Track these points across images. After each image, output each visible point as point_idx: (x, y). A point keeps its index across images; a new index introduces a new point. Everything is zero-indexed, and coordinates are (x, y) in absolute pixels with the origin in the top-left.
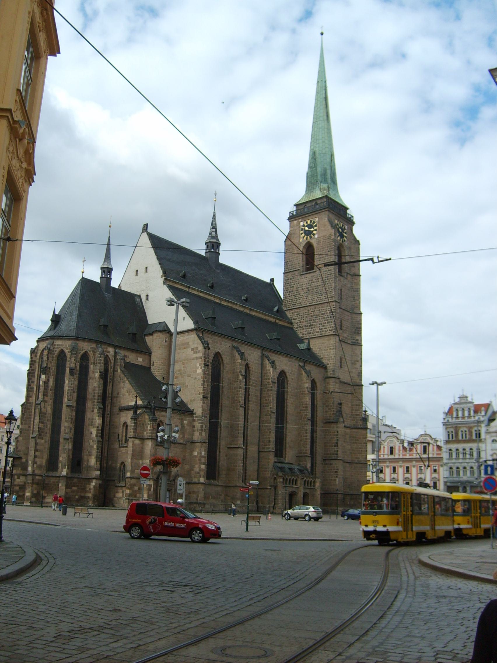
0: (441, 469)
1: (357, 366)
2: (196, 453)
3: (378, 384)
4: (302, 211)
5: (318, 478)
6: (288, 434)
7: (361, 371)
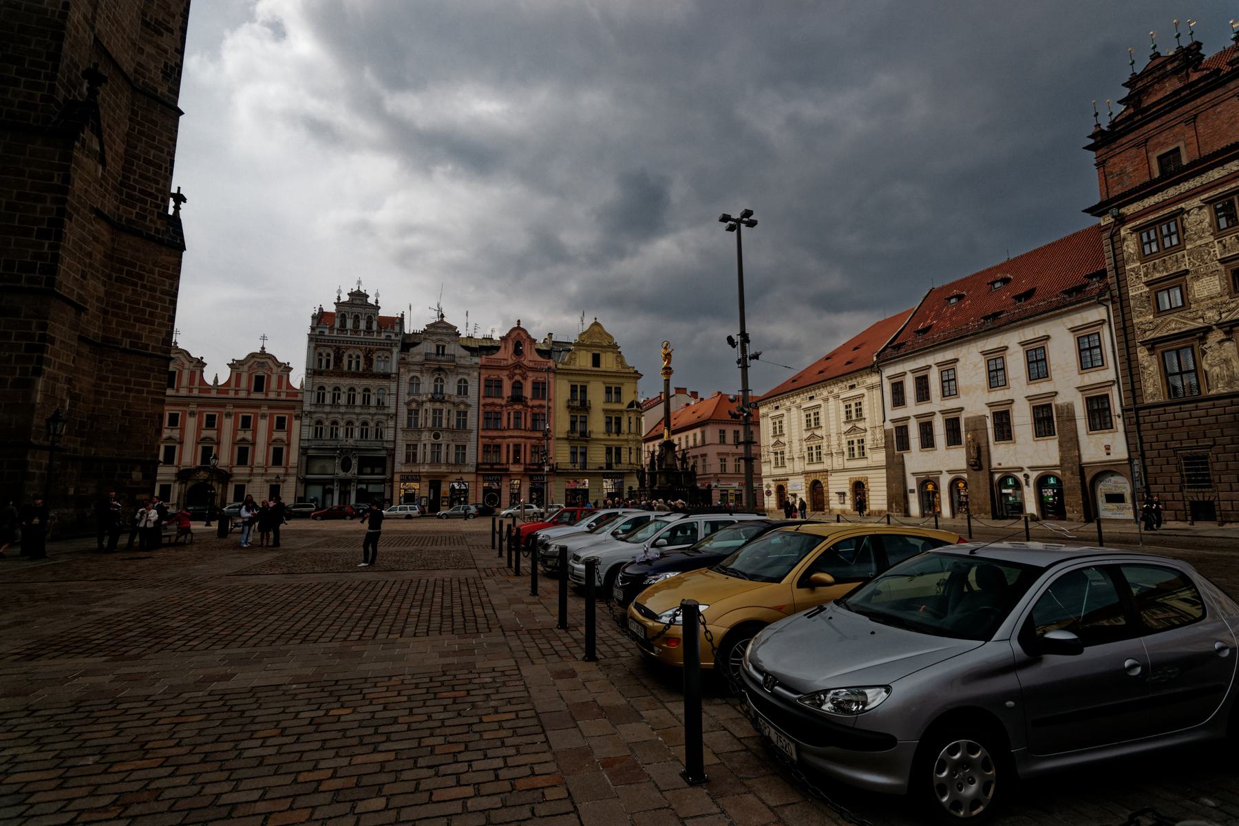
7: (179, 66)
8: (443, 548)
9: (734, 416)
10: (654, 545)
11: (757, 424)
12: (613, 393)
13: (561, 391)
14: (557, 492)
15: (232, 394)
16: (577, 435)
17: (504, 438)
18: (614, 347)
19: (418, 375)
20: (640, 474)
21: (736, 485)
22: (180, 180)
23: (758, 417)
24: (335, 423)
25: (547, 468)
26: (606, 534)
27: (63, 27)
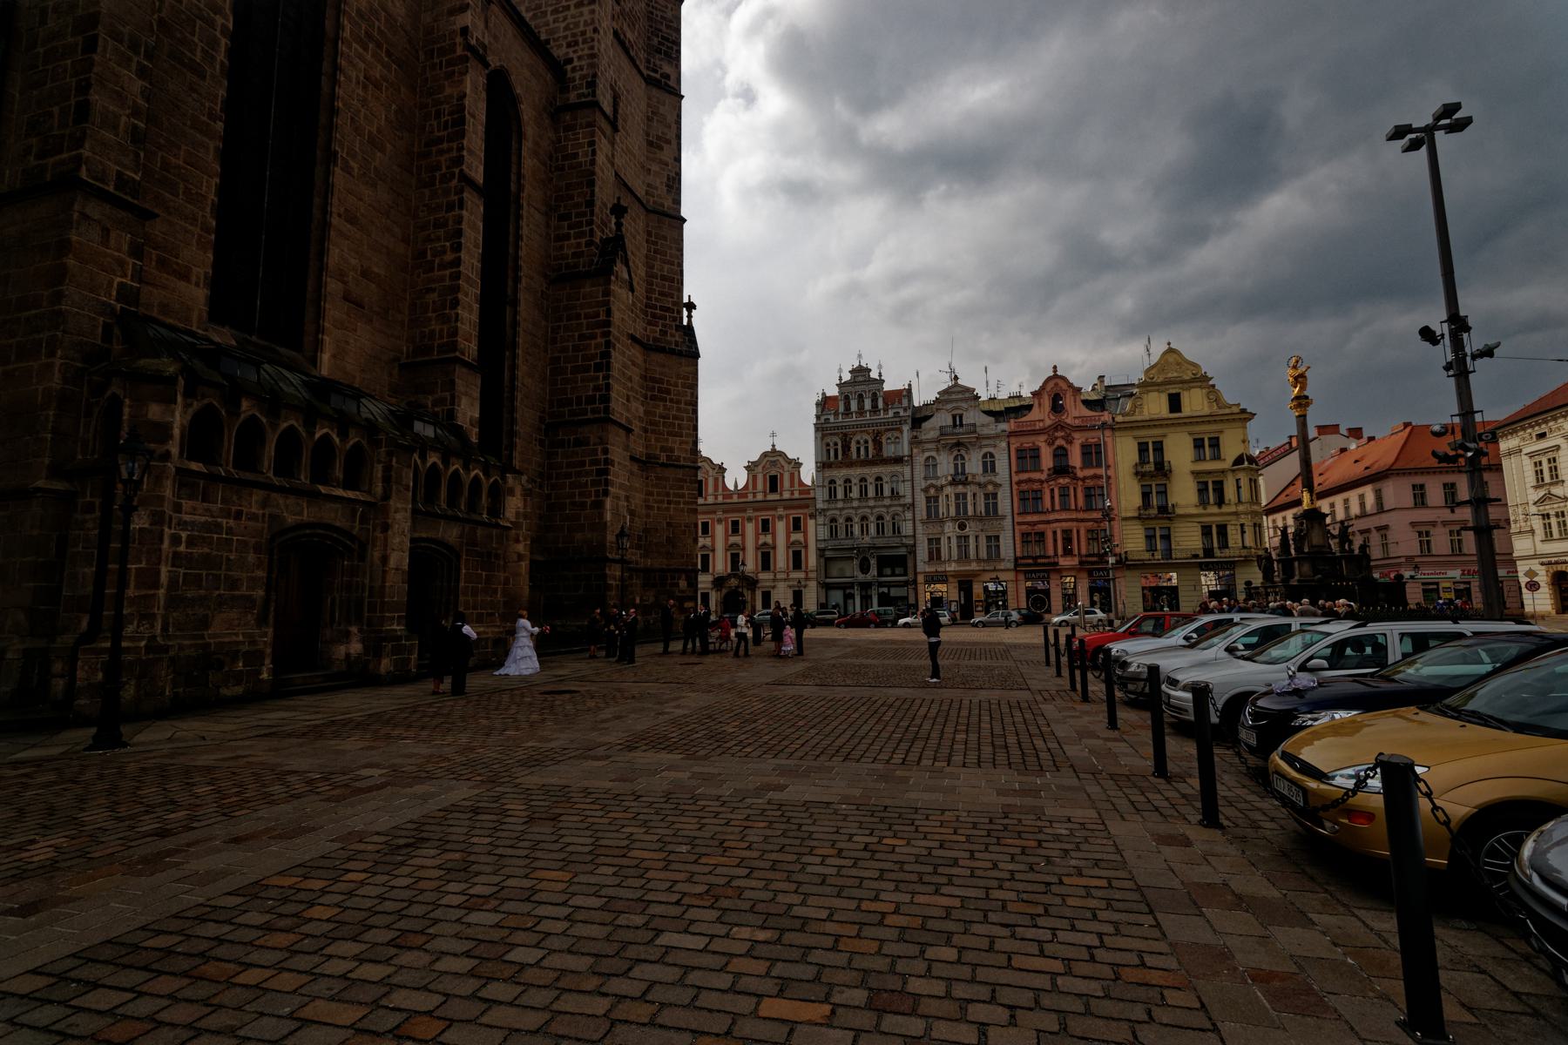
0: (811, 523)
1: (666, 155)
5: (519, 473)
6: (335, 220)
7: (679, 174)
8: (983, 663)
9: (1444, 458)
10: (1303, 668)
11: (1498, 468)
12: (1207, 446)
13: (1124, 453)
14: (1129, 593)
15: (750, 498)
16: (1154, 512)
17: (1048, 522)
18: (1202, 380)
19: (933, 454)
20: (1265, 562)
21: (1456, 573)
22: (690, 290)
23: (1498, 456)
24: (849, 519)
25: (1111, 560)
26: (1216, 648)
27: (593, 173)
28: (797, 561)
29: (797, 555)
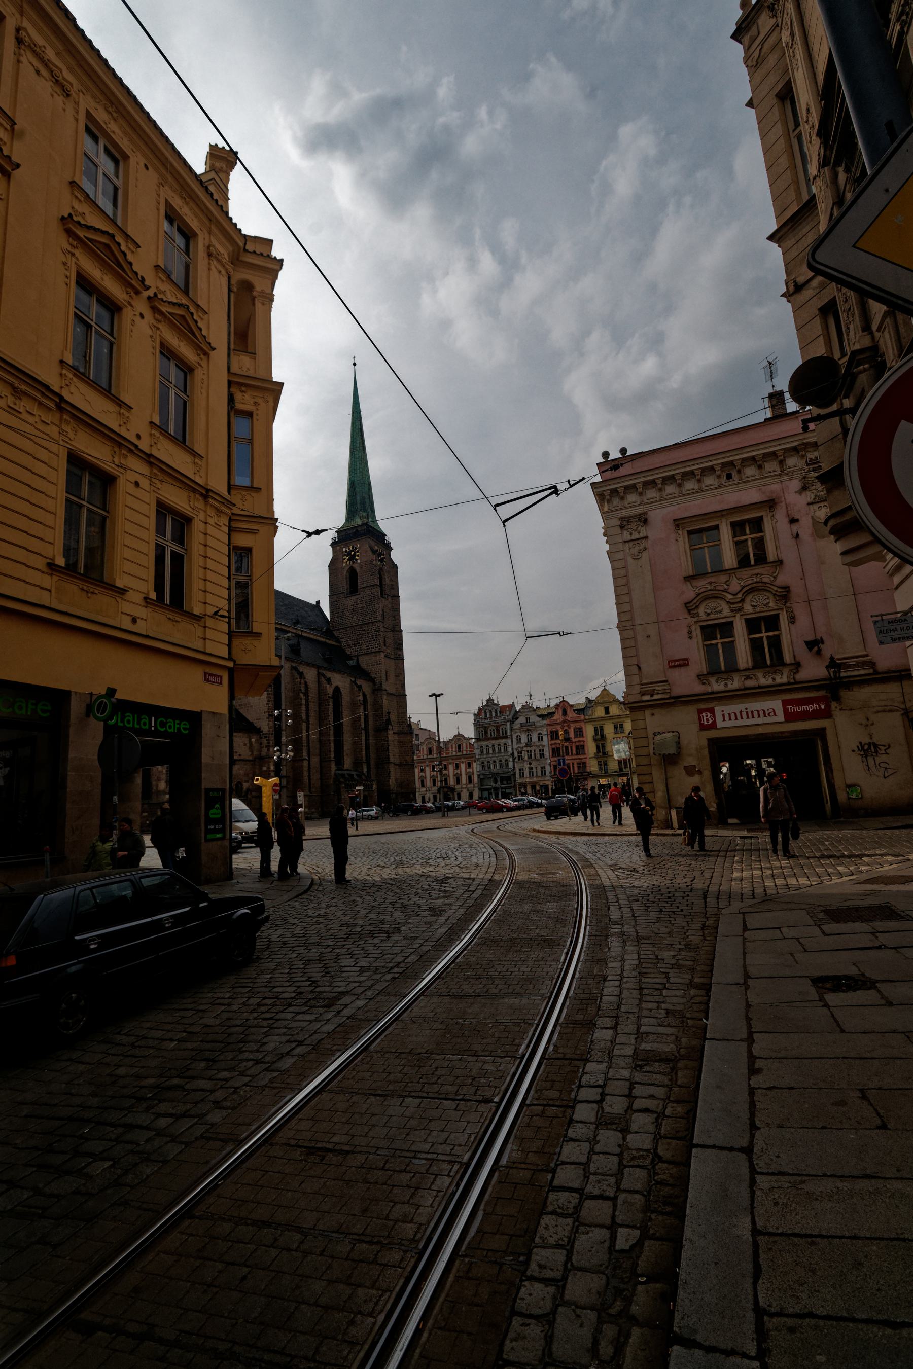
0: (475, 764)
2: (265, 768)
3: (437, 696)
4: (343, 538)
13: (589, 731)
28: (470, 780)
29: (470, 778)
